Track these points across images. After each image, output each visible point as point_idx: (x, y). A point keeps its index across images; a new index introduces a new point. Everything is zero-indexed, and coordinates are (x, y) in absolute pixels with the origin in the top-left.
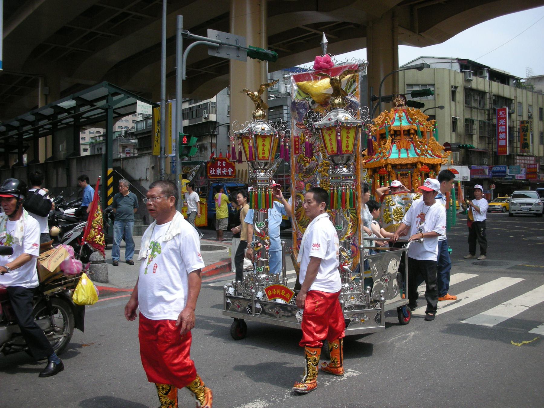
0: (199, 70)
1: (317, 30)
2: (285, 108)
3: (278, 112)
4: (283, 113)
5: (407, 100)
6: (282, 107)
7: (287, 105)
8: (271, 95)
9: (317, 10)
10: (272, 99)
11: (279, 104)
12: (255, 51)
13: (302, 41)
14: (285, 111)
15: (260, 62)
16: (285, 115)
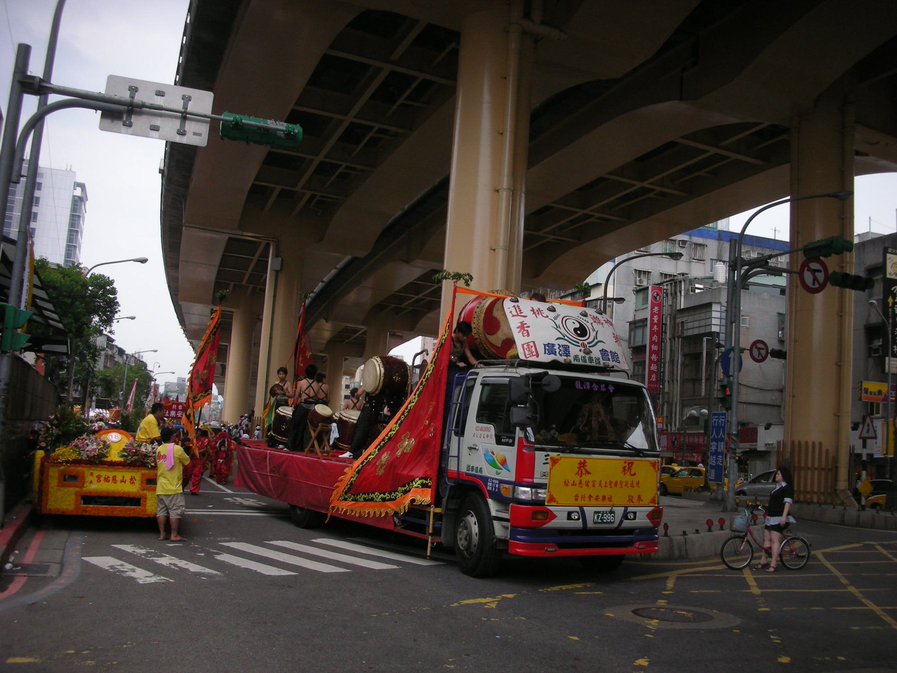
0: (540, 233)
1: (718, 147)
2: (715, 307)
3: (703, 316)
4: (711, 318)
5: (830, 271)
6: (709, 306)
7: (719, 303)
8: (697, 286)
9: (681, 99)
10: (697, 291)
11: (706, 300)
12: (231, 122)
13: (702, 173)
14: (714, 314)
15: (498, 191)
16: (714, 321)
